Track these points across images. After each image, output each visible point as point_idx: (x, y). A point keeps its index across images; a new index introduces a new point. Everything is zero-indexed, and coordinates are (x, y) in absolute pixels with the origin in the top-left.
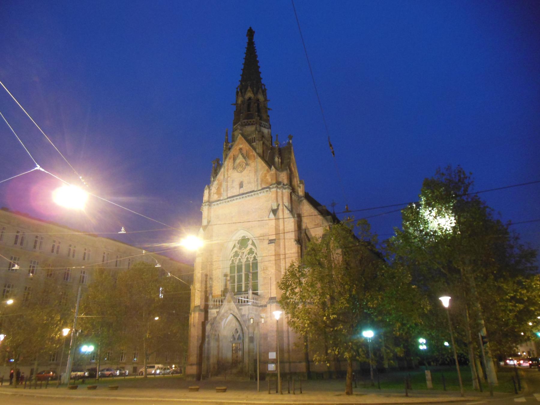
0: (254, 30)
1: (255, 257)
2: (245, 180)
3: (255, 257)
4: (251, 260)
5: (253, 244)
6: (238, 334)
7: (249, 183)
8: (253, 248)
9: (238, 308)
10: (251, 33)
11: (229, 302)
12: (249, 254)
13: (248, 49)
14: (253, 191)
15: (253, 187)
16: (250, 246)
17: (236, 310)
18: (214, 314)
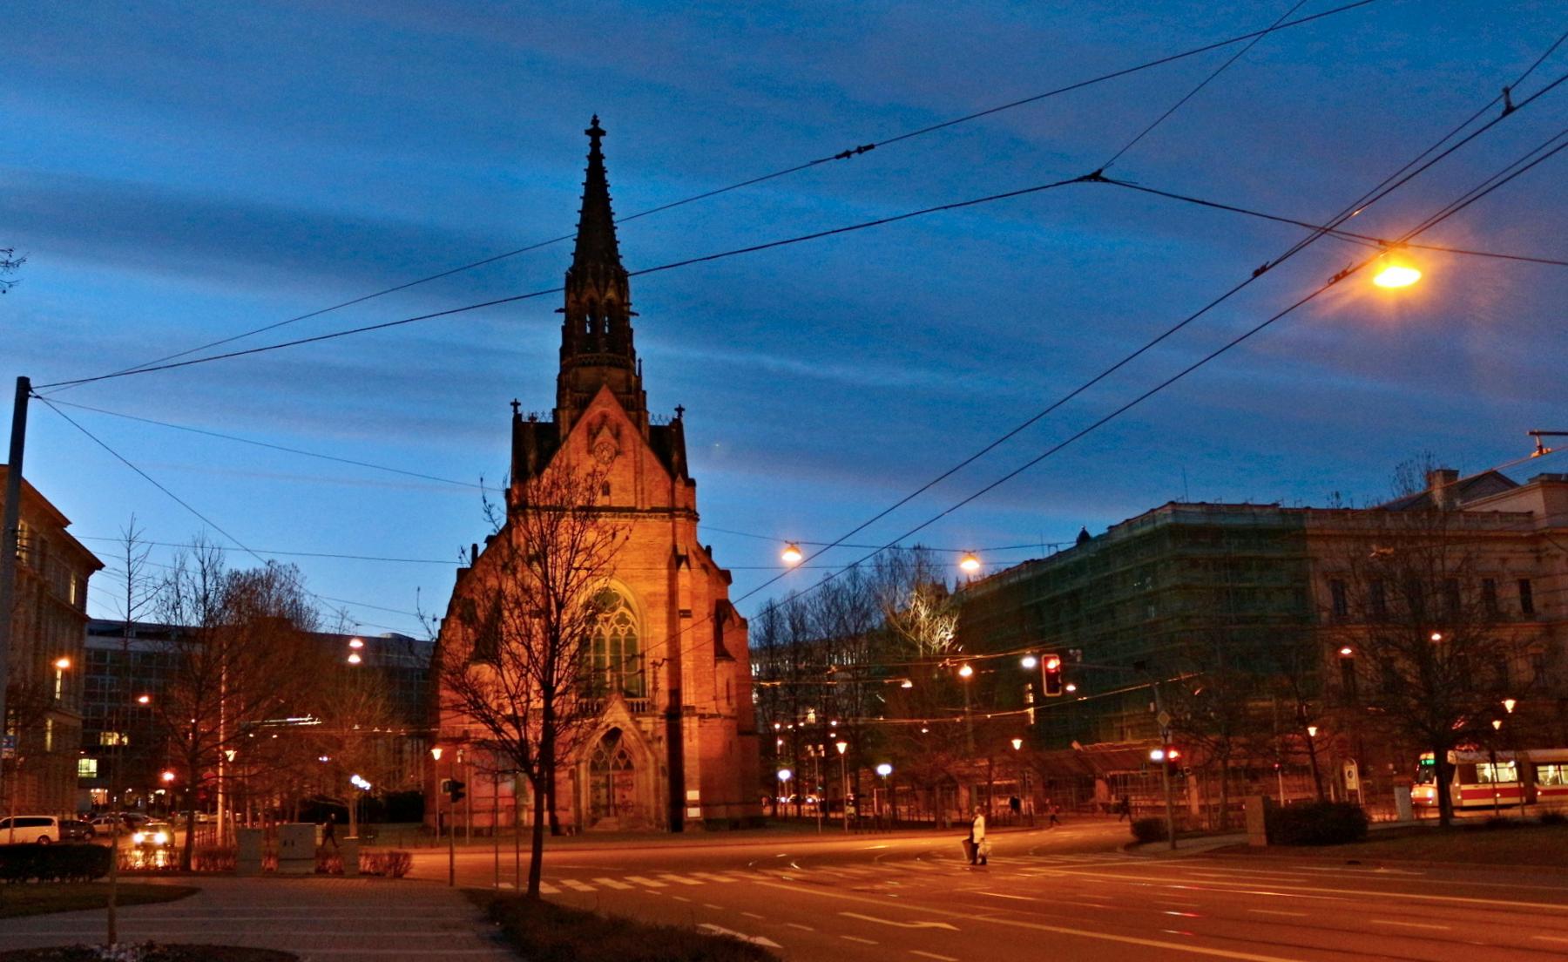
0: (601, 126)
1: (630, 631)
2: (614, 479)
3: (630, 631)
4: (622, 635)
5: (627, 605)
7: (623, 489)
8: (627, 612)
9: (632, 719)
10: (595, 133)
12: (618, 622)
13: (589, 172)
14: (632, 510)
15: (628, 500)
16: (622, 609)
17: (630, 725)
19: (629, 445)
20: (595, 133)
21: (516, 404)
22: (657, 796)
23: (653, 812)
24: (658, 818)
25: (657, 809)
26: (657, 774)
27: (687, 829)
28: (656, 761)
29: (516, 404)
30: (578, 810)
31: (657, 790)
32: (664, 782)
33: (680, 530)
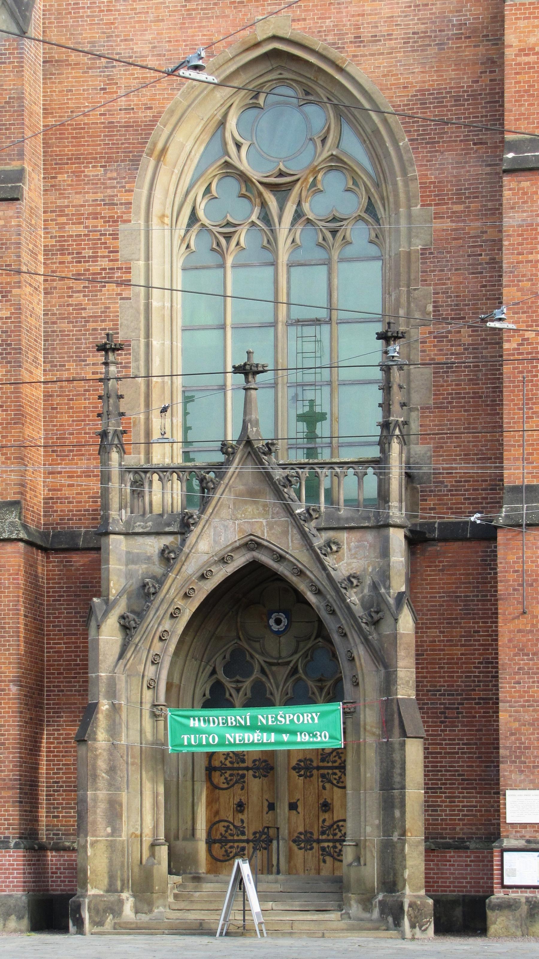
6: (247, 684)
23: (371, 871)
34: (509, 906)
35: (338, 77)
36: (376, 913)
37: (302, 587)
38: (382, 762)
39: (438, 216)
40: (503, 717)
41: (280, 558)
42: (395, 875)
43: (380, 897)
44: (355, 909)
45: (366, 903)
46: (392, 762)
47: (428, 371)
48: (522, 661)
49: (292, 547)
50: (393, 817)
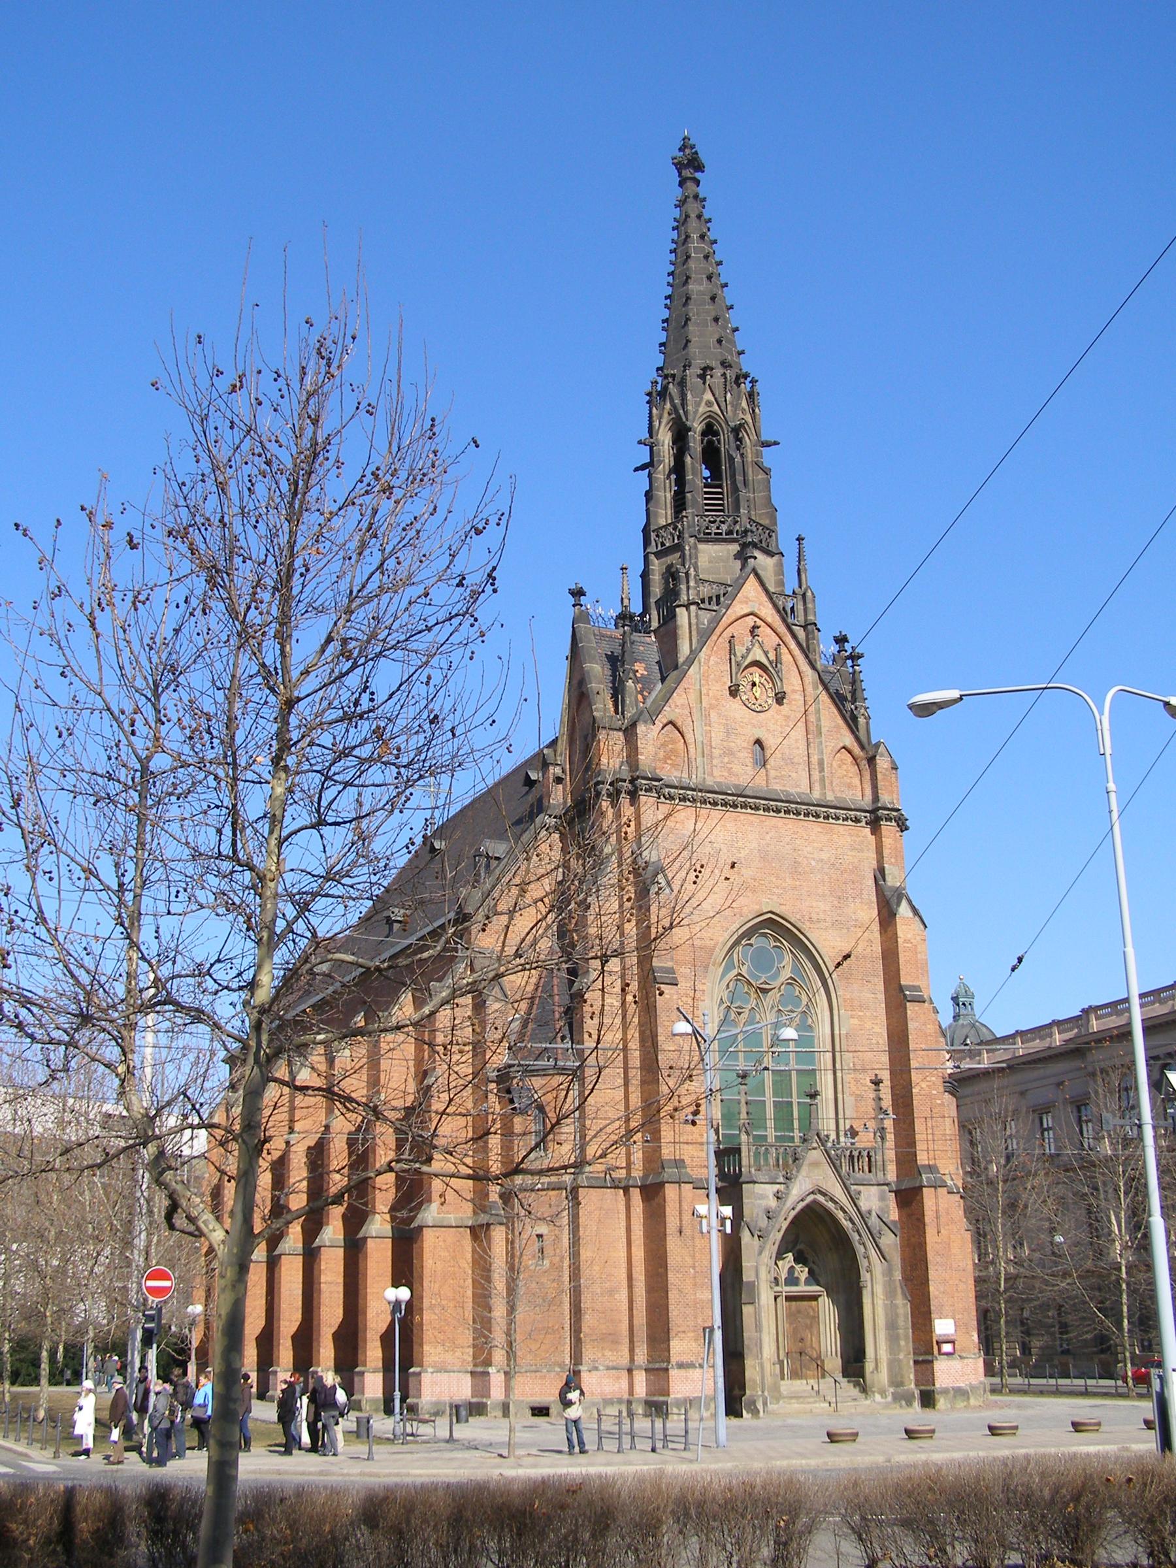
10: (689, 164)
11: (816, 1164)
17: (838, 1192)
18: (763, 1197)
19: (791, 683)
20: (689, 164)
21: (578, 593)
22: (893, 1339)
23: (883, 1376)
24: (896, 1382)
25: (894, 1364)
26: (890, 1294)
27: (941, 1403)
28: (889, 1272)
29: (578, 593)
30: (762, 1366)
31: (891, 1326)
32: (904, 1308)
33: (887, 842)
34: (945, 1391)
35: (801, 937)
36: (890, 1398)
37: (840, 1215)
38: (887, 1315)
39: (852, 1017)
40: (931, 1289)
41: (832, 1200)
42: (902, 1377)
43: (892, 1390)
44: (878, 1397)
45: (883, 1393)
46: (897, 1315)
47: (853, 1098)
48: (938, 1259)
49: (838, 1192)
50: (899, 1345)
